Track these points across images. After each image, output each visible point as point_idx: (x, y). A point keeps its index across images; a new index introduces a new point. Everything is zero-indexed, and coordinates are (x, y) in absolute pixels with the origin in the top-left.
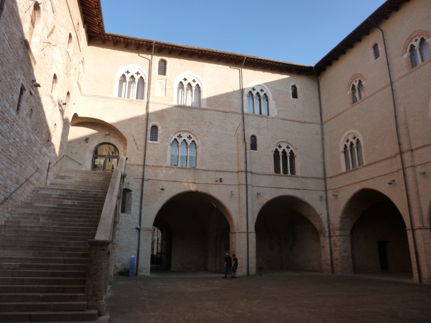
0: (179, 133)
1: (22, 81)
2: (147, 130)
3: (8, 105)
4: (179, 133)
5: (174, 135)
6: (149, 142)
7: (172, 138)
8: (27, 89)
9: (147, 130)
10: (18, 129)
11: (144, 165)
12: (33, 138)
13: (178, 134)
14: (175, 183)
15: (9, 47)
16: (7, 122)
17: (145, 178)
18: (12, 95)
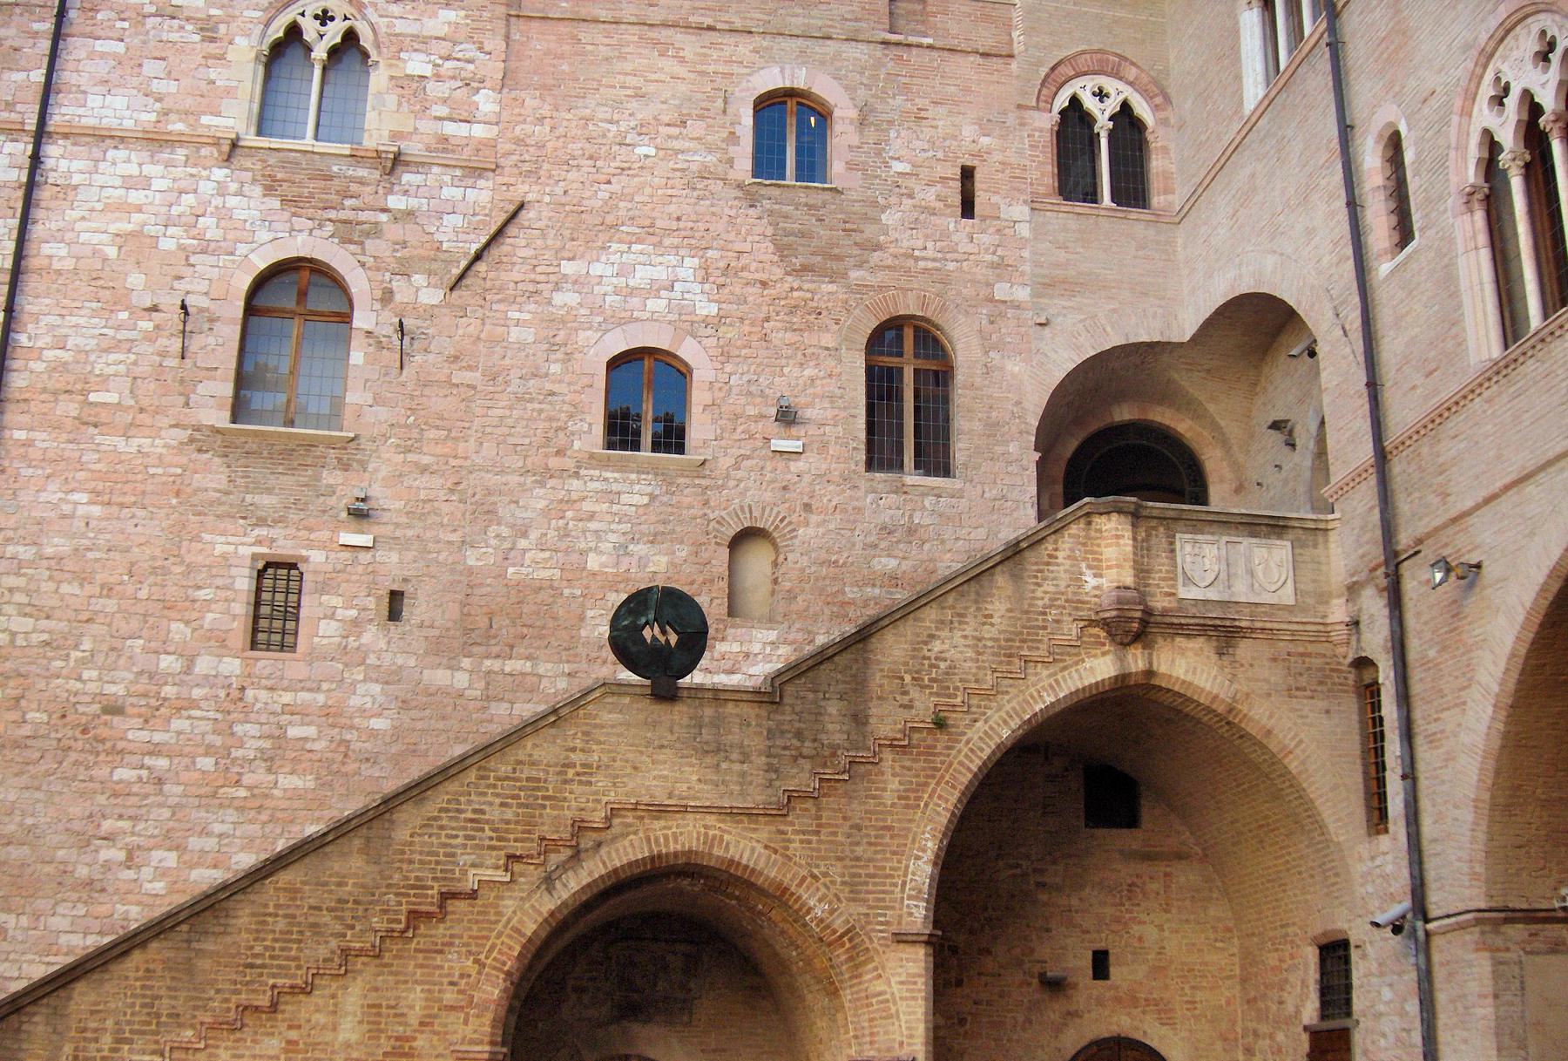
0: (1489, 77)
1: (246, 551)
2: (1353, 205)
3: (168, 663)
4: (1489, 77)
5: (1466, 113)
6: (1382, 269)
7: (1462, 148)
8: (304, 553)
9: (1353, 205)
10: (287, 698)
11: (1382, 456)
12: (461, 680)
13: (1487, 90)
14: (1530, 489)
15: (115, 509)
16: (179, 709)
17: (1404, 539)
18: (187, 623)
